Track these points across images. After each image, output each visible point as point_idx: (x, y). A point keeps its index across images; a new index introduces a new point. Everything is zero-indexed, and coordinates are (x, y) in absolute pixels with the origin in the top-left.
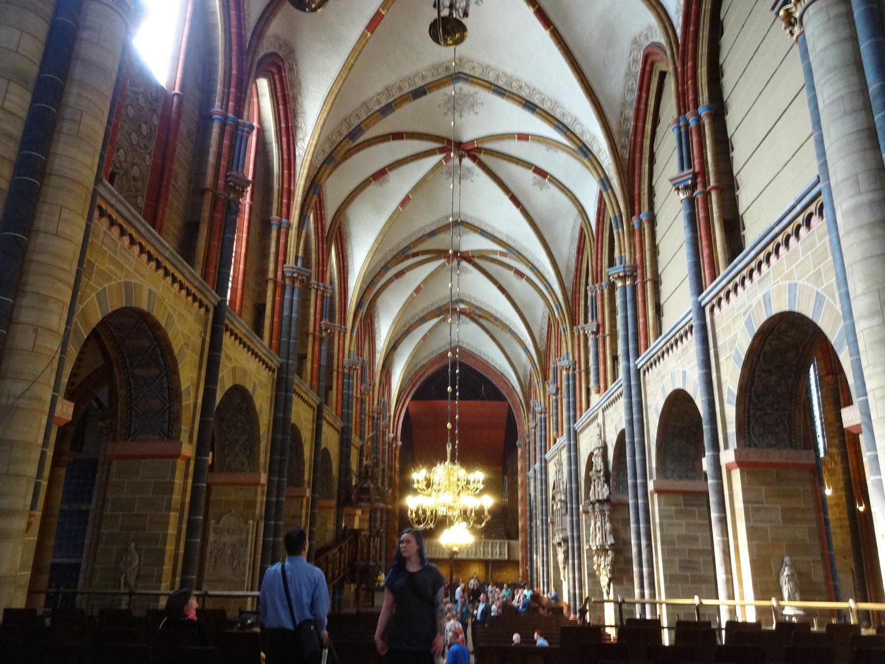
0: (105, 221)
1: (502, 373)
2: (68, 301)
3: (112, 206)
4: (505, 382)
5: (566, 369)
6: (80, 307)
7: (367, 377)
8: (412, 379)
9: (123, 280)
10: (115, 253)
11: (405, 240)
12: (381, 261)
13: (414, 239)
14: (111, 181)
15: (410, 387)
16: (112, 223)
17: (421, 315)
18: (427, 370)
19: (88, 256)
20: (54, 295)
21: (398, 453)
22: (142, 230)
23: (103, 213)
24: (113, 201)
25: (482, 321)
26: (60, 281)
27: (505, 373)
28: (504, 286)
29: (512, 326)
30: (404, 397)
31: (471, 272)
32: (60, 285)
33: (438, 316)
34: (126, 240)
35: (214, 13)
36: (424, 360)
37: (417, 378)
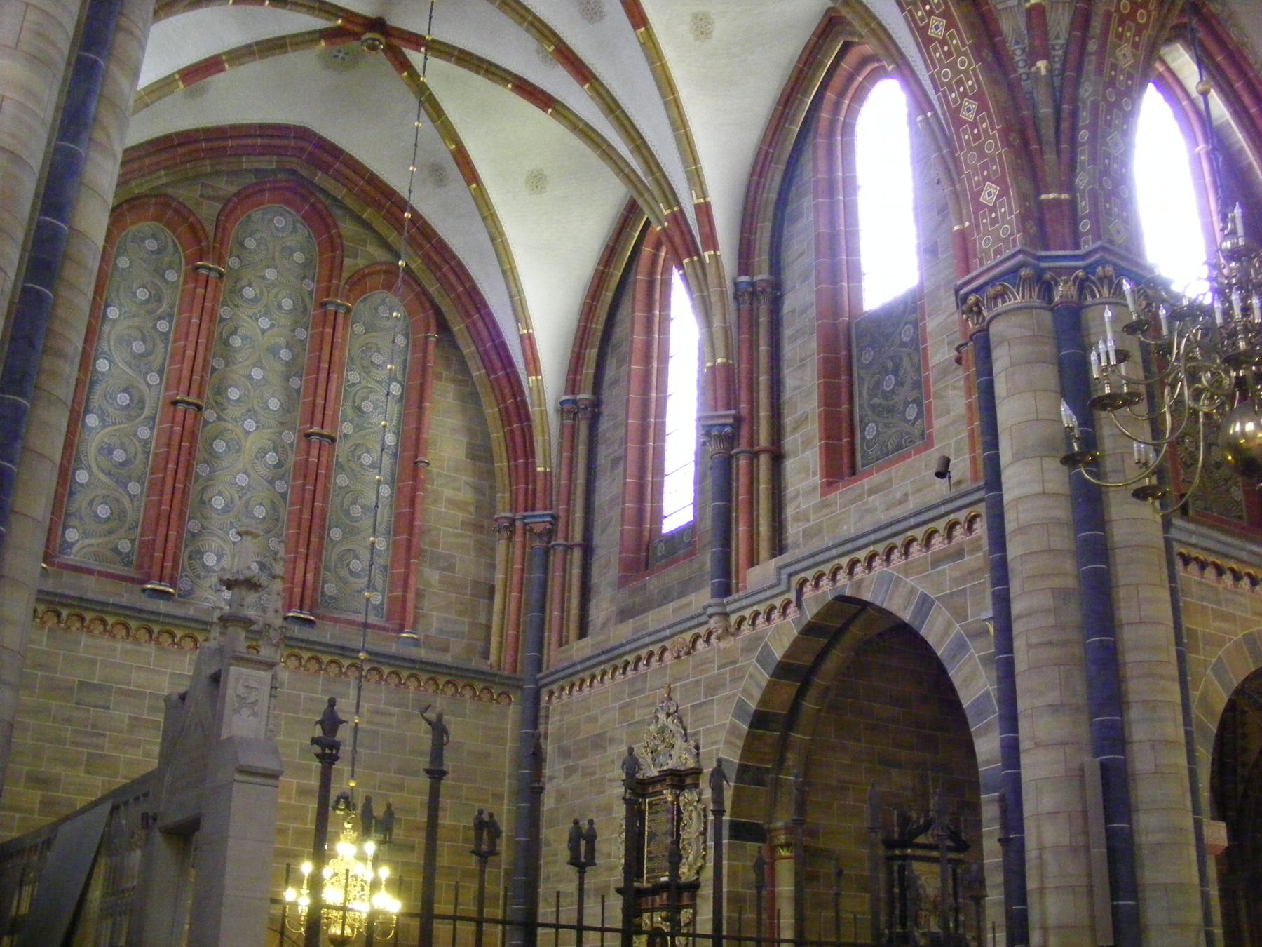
0: (1193, 567)
2: (1177, 697)
3: (1195, 546)
6: (1195, 695)
9: (1240, 635)
10: (1219, 603)
14: (1184, 511)
16: (1203, 566)
19: (1186, 624)
20: (1159, 697)
22: (1244, 556)
23: (1186, 560)
24: (1193, 540)
26: (1162, 677)
32: (1162, 682)
34: (1228, 578)
35: (1241, 150)
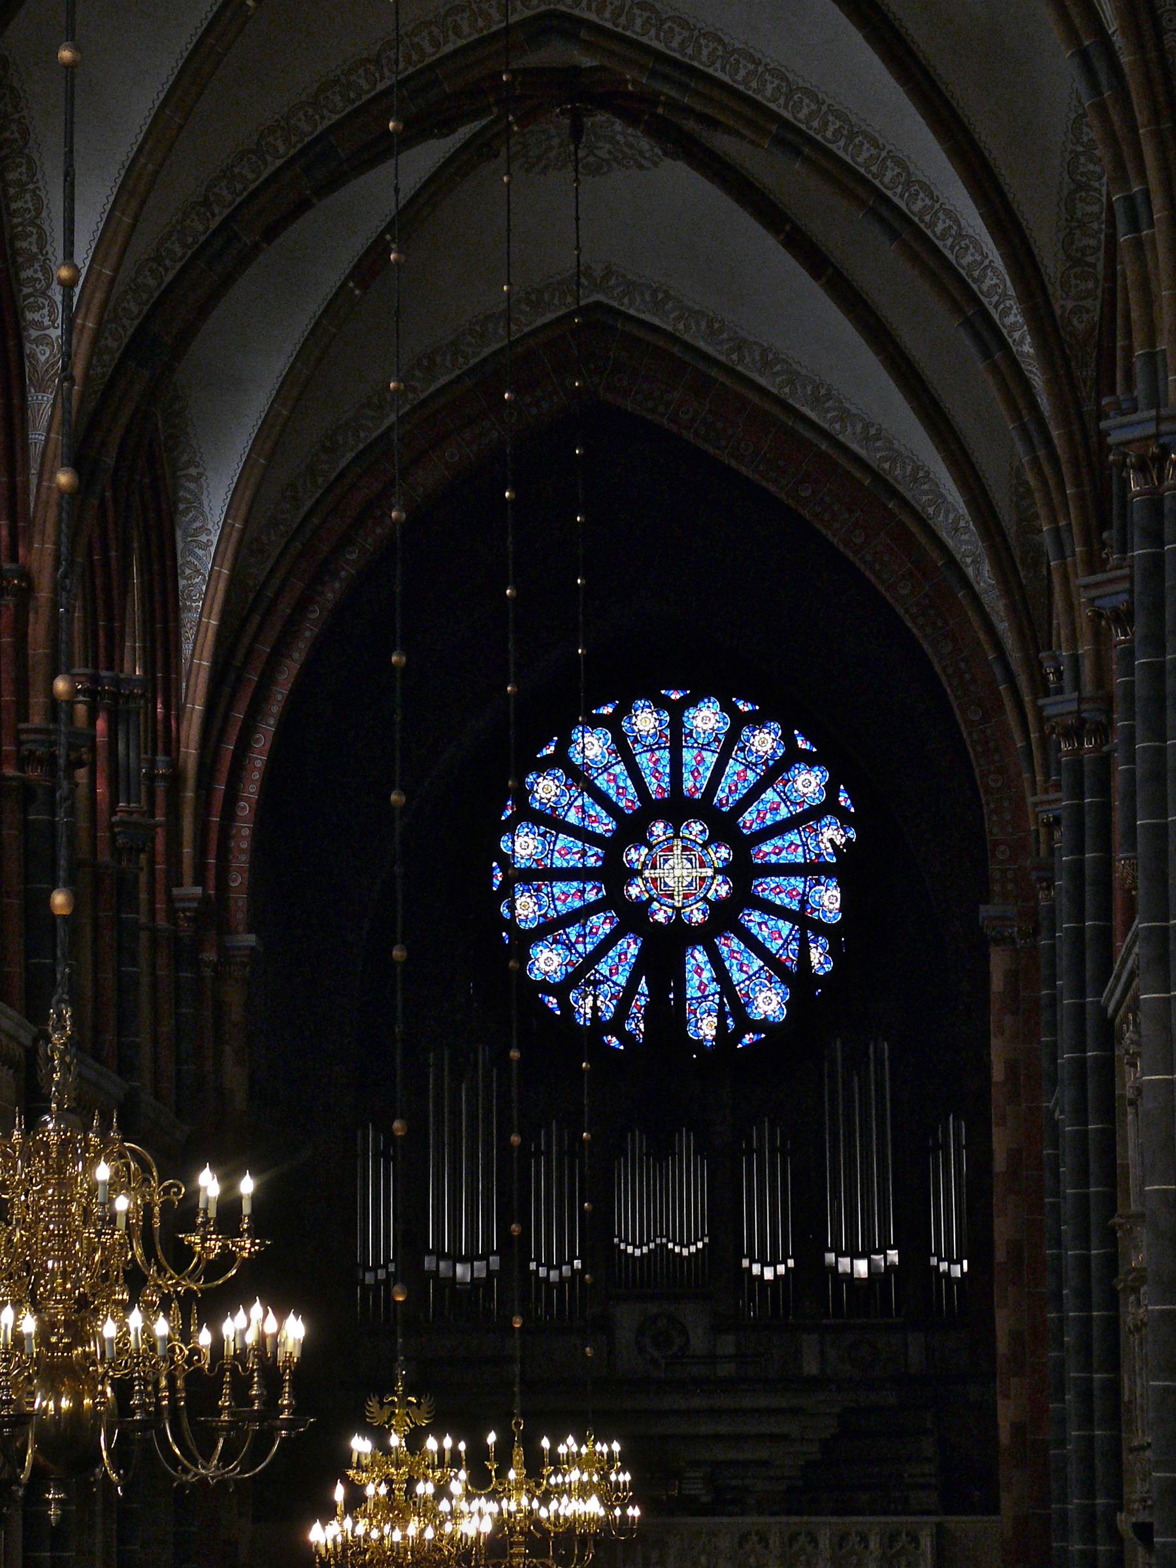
1: (878, 478)
5: (1142, 468)
21: (234, 997)
27: (898, 474)
29: (887, 180)
33: (447, 126)
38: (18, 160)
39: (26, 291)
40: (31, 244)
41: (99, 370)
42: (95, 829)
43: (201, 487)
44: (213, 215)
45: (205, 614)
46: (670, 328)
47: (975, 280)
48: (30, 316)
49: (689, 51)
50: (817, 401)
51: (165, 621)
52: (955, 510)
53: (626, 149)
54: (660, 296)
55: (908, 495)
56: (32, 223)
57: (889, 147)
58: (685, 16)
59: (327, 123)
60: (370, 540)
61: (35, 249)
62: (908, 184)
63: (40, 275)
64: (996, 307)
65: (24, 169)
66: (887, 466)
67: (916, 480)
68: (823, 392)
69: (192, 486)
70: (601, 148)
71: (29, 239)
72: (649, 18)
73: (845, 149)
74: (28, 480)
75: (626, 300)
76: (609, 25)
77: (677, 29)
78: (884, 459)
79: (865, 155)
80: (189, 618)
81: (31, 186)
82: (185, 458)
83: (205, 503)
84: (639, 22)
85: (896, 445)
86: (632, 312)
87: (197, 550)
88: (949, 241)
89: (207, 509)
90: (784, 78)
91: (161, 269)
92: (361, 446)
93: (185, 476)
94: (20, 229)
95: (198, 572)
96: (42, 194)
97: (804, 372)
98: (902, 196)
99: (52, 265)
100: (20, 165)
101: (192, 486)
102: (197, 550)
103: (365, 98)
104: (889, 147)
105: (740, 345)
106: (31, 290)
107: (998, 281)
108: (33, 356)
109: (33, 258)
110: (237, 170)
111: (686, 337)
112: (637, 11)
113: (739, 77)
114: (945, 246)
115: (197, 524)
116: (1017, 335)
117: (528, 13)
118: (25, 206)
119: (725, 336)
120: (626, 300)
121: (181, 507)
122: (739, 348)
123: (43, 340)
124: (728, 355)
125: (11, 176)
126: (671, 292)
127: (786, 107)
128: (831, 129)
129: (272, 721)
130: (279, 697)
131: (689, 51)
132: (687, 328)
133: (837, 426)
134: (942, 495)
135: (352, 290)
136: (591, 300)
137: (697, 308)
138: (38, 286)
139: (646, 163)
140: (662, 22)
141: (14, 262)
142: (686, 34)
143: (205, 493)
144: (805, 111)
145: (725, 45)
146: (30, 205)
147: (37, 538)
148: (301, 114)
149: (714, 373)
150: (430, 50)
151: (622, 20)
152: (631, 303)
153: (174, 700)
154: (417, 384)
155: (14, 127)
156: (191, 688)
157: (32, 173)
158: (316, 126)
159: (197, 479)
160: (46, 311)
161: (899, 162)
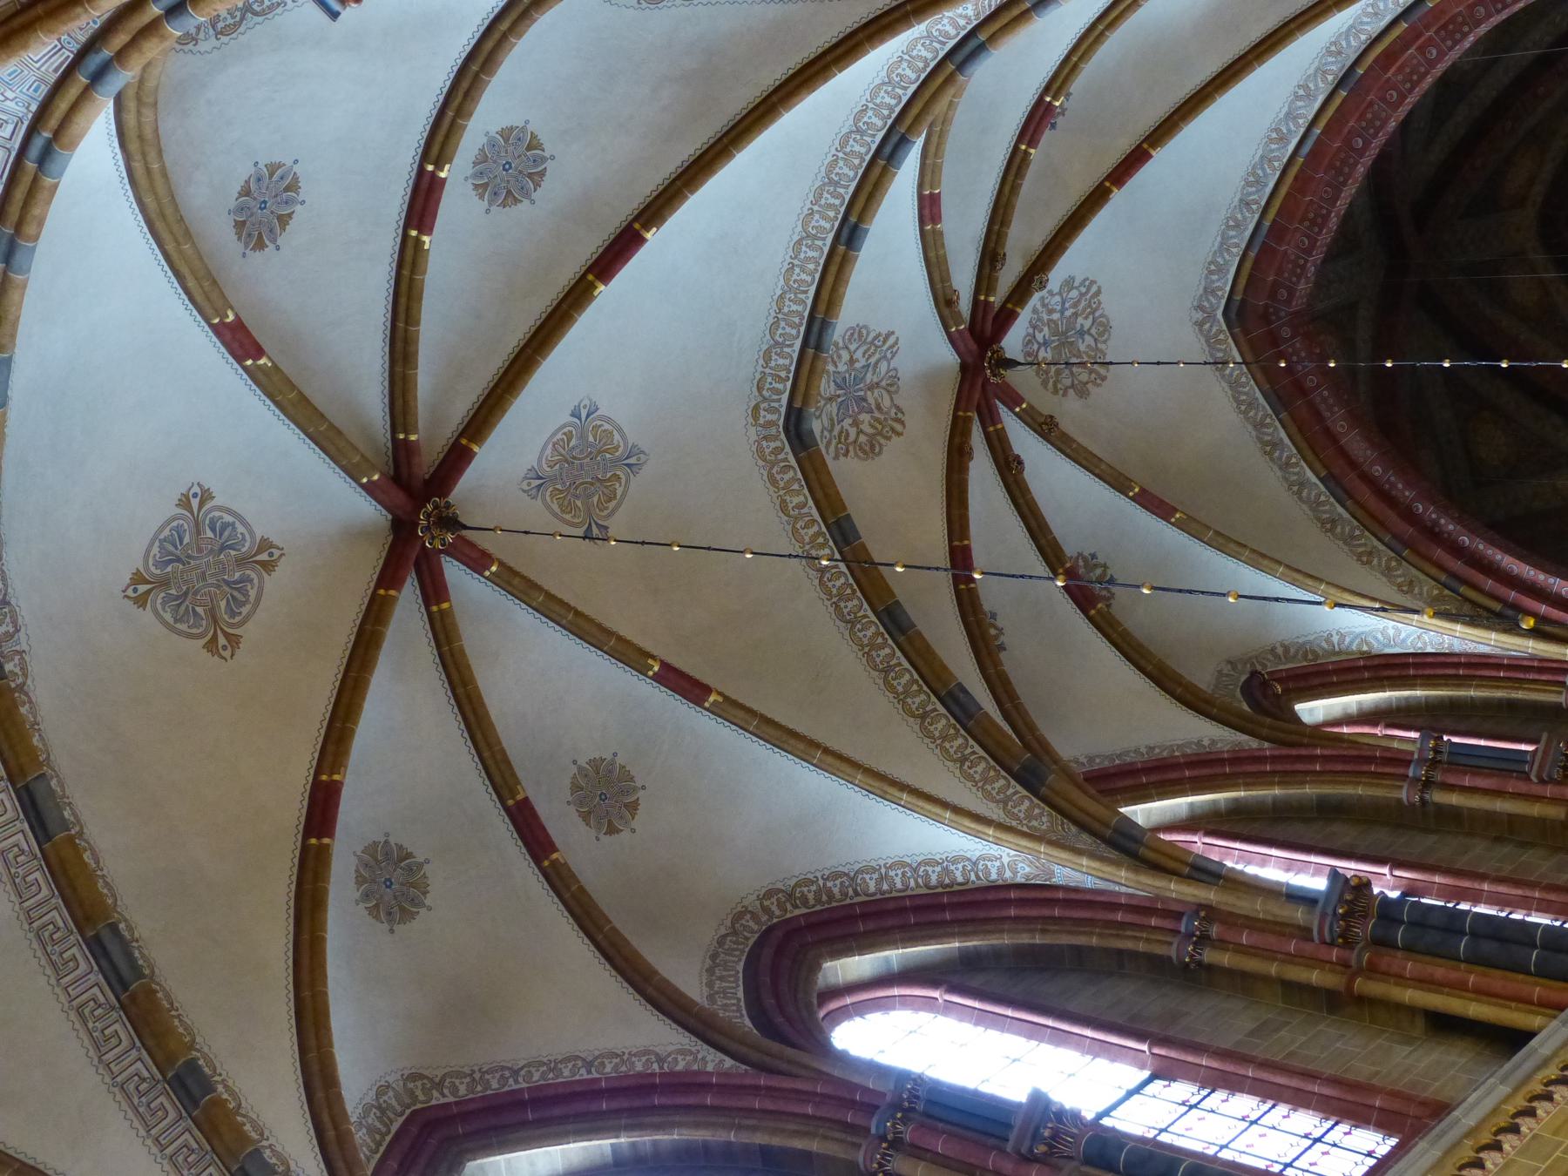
1: (1341, 83)
4: (1388, 57)
7: (1159, 950)
8: (1400, 545)
11: (58, 969)
12: (146, 1119)
13: (59, 916)
15: (1439, 554)
17: (872, 627)
18: (1353, 464)
25: (1023, 240)
27: (1336, 68)
28: (590, 246)
30: (1489, 584)
31: (584, 414)
36: (1302, 484)
37: (1391, 517)
38: (859, 881)
39: (973, 877)
40: (934, 872)
41: (1044, 819)
42: (1544, 798)
43: (1351, 633)
44: (935, 710)
45: (1453, 634)
46: (1238, 259)
47: (927, 65)
48: (994, 876)
49: (797, 320)
50: (1282, 139)
51: (1457, 665)
52: (1359, 17)
53: (1080, 308)
54: (1213, 267)
55: (1353, 57)
56: (915, 870)
57: (834, 152)
58: (768, 325)
59: (870, 613)
60: (1407, 493)
61: (938, 869)
62: (858, 131)
63: (960, 866)
64: (944, 44)
65: (867, 877)
66: (1330, 78)
67: (1340, 53)
68: (1274, 135)
69: (1348, 640)
70: (1082, 325)
71: (930, 872)
72: (776, 353)
73: (847, 187)
74: (1126, 894)
75: (1220, 293)
76: (789, 384)
77: (780, 331)
78: (1324, 80)
79: (846, 170)
80: (1458, 646)
81: (883, 871)
82: (1324, 645)
83: (1361, 630)
84: (781, 361)
85: (1311, 71)
86: (1228, 288)
87: (1401, 637)
88: (900, 91)
89: (1367, 629)
90: (799, 242)
91: (972, 758)
92: (1332, 500)
93: (1339, 645)
94: (920, 880)
95: (1419, 637)
96: (890, 861)
97: (1260, 152)
98: (874, 136)
99: (951, 856)
100: (863, 879)
101: (1348, 640)
102: (1401, 637)
103: (851, 581)
104: (834, 152)
105: (1245, 203)
106: (972, 874)
107: (919, 45)
108: (1027, 877)
109: (946, 870)
110: (900, 689)
111: (1243, 246)
112: (773, 364)
113: (809, 279)
114: (905, 94)
115: (1380, 636)
116: (962, 22)
117: (787, 448)
118: (900, 876)
119: (1239, 216)
120: (1220, 293)
121: (1365, 648)
122: (1248, 204)
123: (1013, 867)
124: (1253, 212)
125: (872, 887)
126: (1209, 259)
127: (824, 239)
128: (832, 201)
129: (1551, 580)
130: (1532, 573)
131: (797, 320)
132: (1237, 246)
133: (1301, 121)
134: (1349, 29)
135: (1177, 519)
136: (1222, 320)
137: (1219, 239)
138: (969, 868)
139: (1094, 289)
140: (777, 343)
141: (947, 886)
142: (783, 324)
143: (1353, 629)
144: (823, 223)
145: (784, 293)
146: (899, 872)
147: (1168, 894)
148: (861, 635)
149: (1267, 223)
150: (815, 528)
151: (783, 374)
152: (1221, 289)
153: (1525, 663)
154: (1285, 455)
155: (829, 884)
156: (1515, 648)
157: (874, 870)
158: (872, 622)
159: (1342, 636)
160: (989, 864)
161: (844, 142)
